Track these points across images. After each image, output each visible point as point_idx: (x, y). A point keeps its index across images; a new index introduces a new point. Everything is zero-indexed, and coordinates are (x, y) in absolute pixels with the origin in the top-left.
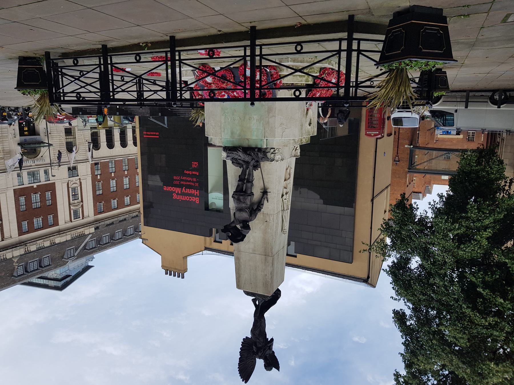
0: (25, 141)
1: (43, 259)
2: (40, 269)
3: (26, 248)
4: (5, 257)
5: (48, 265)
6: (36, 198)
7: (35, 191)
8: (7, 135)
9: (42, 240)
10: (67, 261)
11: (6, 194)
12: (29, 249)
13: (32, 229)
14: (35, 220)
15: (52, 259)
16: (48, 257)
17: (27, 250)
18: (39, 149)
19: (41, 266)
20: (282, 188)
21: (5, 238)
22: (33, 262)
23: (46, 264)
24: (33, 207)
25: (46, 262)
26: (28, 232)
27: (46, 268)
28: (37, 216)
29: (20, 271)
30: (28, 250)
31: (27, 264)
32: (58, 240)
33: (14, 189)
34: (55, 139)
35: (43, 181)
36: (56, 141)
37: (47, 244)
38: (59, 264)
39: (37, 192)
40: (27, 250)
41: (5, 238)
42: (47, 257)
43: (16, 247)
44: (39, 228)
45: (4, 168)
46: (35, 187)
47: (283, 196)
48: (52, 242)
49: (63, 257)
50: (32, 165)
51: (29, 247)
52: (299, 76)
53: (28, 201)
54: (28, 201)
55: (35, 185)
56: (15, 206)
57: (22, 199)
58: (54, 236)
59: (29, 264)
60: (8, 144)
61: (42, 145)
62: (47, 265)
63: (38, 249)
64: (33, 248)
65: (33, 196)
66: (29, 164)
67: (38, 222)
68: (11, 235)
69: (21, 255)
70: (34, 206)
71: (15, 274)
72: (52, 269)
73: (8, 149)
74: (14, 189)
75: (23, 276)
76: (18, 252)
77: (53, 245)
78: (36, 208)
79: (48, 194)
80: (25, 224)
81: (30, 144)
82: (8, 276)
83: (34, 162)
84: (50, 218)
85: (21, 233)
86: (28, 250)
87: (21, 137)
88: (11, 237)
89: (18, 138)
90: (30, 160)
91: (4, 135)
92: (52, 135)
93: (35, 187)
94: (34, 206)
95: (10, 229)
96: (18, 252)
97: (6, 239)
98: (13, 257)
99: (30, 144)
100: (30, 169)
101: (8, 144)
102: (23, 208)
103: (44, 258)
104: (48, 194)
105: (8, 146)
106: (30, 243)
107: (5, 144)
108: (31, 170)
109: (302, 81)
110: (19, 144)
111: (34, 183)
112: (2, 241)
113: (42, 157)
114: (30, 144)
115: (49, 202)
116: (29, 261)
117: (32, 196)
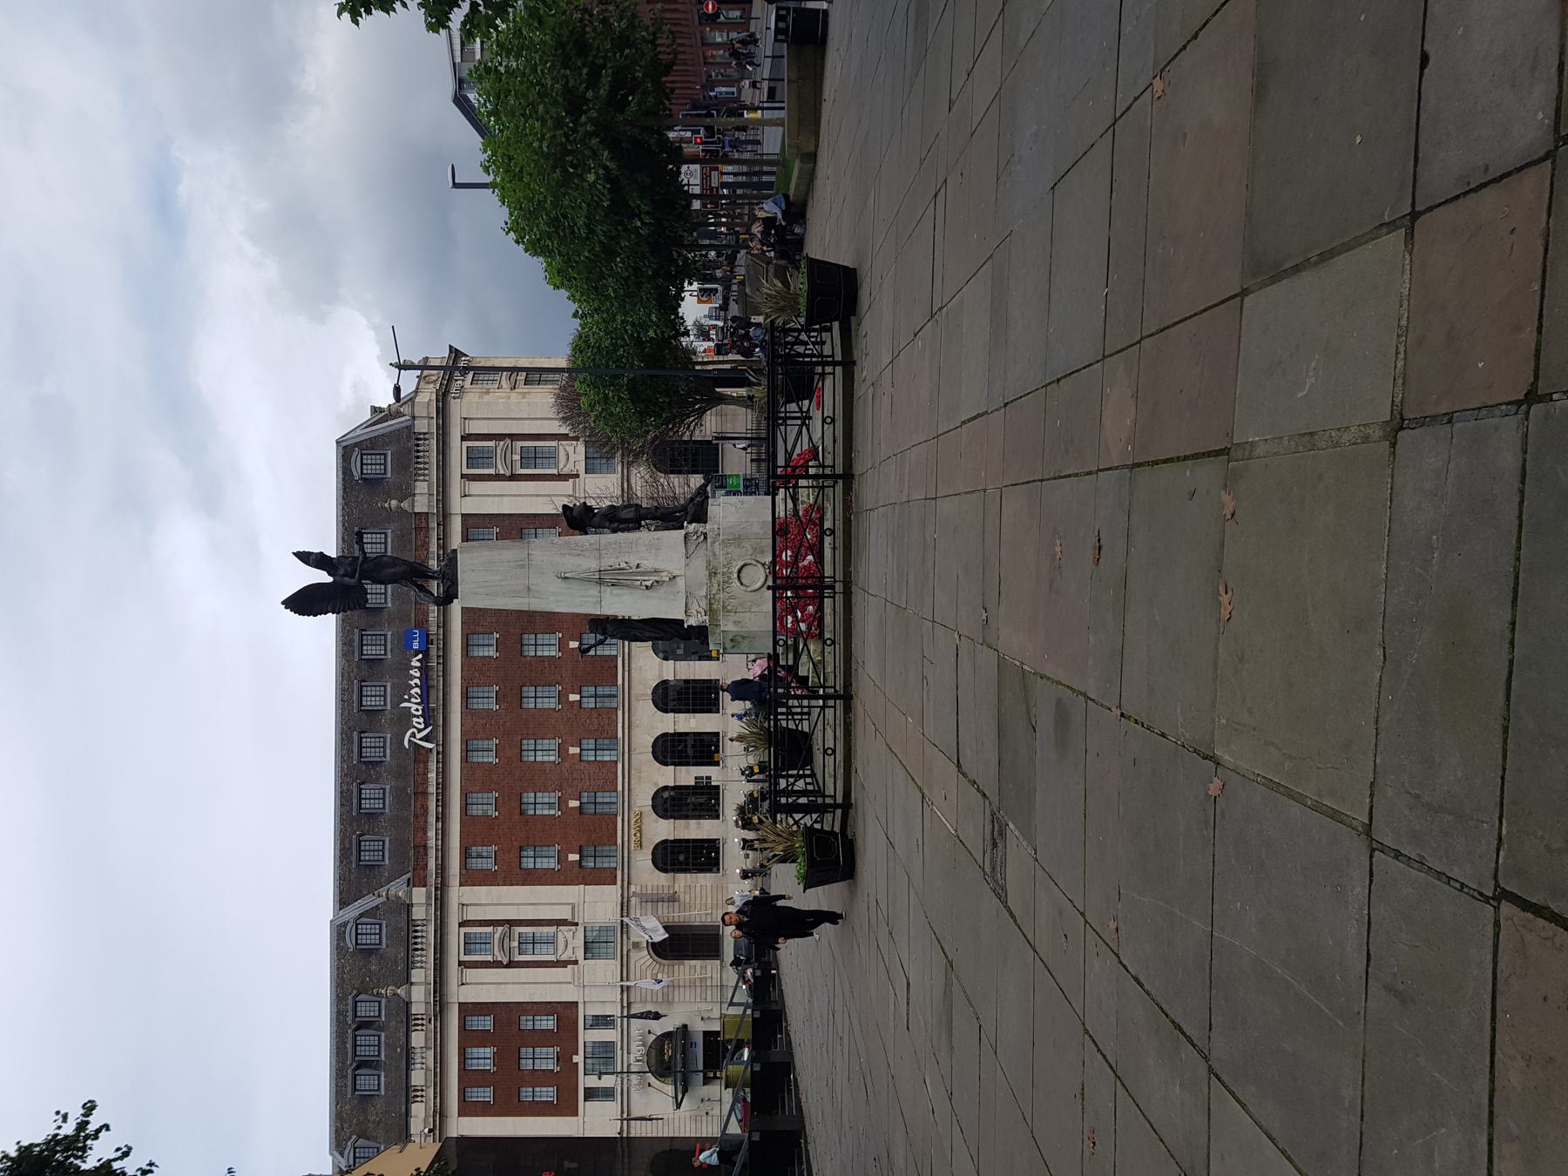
0: (692, 1043)
1: (376, 1072)
2: (353, 1060)
3: (424, 1022)
4: (419, 965)
5: (355, 1084)
6: (545, 1059)
7: (565, 1059)
8: (709, 999)
9: (432, 1066)
10: (346, 1157)
11: (570, 983)
12: (419, 1028)
13: (468, 1038)
14: (488, 1051)
15: (366, 1099)
16: (379, 1089)
17: (419, 1022)
18: (670, 1080)
19: (358, 1068)
20: (638, 562)
21: (464, 970)
22: (379, 1045)
23: (361, 1081)
24: (523, 1050)
25: (366, 1082)
26: (463, 1027)
27: (350, 1076)
28: (497, 1059)
29: (366, 1010)
30: (418, 1025)
31: (381, 1029)
32: (419, 1111)
33: (577, 1003)
34: (693, 1126)
35: (586, 1081)
36: (688, 1129)
37: (417, 1078)
38: (346, 1126)
39: (560, 1062)
40: (419, 1022)
41: (464, 970)
42: (379, 1085)
43: (435, 992)
44: (465, 1058)
45: (632, 976)
46: (576, 1059)
47: (626, 563)
48: (419, 1093)
49: (363, 1134)
50: (632, 1056)
51: (424, 1028)
52: (809, 494)
53: (543, 1038)
54: (543, 1038)
55: (578, 1059)
56: (536, 1003)
57: (548, 1023)
58: (435, 1098)
59: (378, 1033)
60: (687, 999)
61: (680, 1088)
62: (358, 1082)
63: (408, 1051)
64: (417, 1039)
65: (552, 1051)
66: (634, 1048)
67: (483, 1058)
68: (467, 984)
69: (408, 1004)
70: (526, 1052)
71: (361, 997)
72: (337, 1104)
73: (676, 999)
74: (577, 1003)
75: (350, 1014)
76: (419, 997)
77: (408, 1094)
78: (520, 1058)
79: (547, 1094)
80: (485, 1023)
81: (685, 1055)
82: (362, 982)
83: (638, 1061)
84: (485, 1094)
85: (467, 1010)
86: (418, 1025)
87: (702, 1033)
88: (463, 984)
89: (698, 1027)
90: (644, 1050)
91: (709, 992)
92: (704, 1118)
93: (576, 1059)
94: (526, 1052)
95: (482, 984)
96: (419, 997)
97: (462, 971)
98: (412, 984)
99: (684, 1052)
100: (622, 1048)
101: (687, 999)
102: (527, 1023)
103: (379, 1076)
104: (547, 1094)
105: (682, 999)
106: (435, 1028)
107: (687, 990)
108: (619, 1052)
109: (802, 496)
110: (685, 1026)
111: (585, 1058)
112: (459, 961)
113: (649, 1085)
114: (685, 1055)
115: (527, 1094)
116: (383, 1034)
117: (551, 1050)
